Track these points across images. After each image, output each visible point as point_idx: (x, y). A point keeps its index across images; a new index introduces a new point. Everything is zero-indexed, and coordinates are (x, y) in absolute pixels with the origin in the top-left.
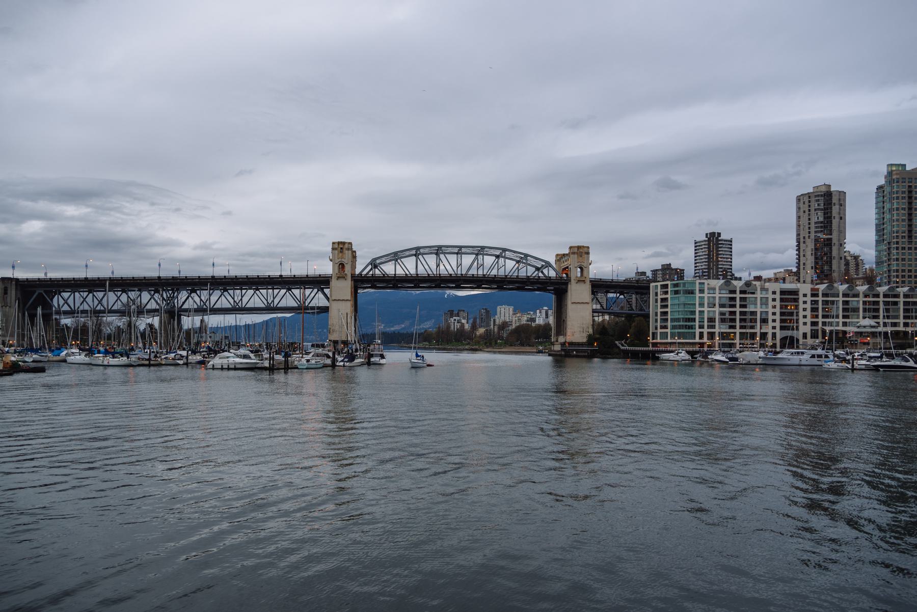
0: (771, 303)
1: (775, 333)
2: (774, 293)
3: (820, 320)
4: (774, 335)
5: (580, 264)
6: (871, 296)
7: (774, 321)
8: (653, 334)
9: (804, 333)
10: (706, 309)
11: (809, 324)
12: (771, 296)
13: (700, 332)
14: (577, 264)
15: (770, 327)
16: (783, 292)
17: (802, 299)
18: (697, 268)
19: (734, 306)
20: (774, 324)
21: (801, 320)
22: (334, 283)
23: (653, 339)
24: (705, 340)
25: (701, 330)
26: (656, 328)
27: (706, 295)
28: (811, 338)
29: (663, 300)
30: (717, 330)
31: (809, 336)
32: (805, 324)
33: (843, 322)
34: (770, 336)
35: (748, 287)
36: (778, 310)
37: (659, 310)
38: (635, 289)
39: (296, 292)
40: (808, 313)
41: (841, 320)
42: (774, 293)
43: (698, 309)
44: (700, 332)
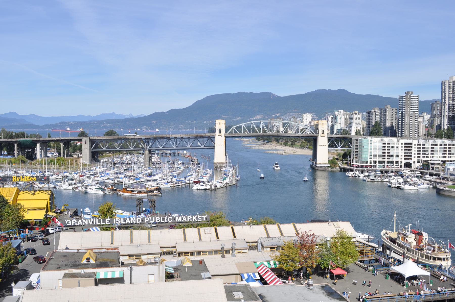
0: (400, 148)
1: (402, 161)
2: (402, 144)
3: (421, 155)
6: (443, 145)
10: (373, 151)
11: (416, 157)
12: (400, 145)
13: (370, 161)
16: (405, 144)
21: (413, 155)
25: (371, 160)
27: (373, 145)
28: (417, 163)
30: (377, 160)
31: (416, 162)
32: (415, 157)
34: (400, 162)
36: (403, 151)
40: (416, 153)
43: (369, 151)
44: (370, 161)
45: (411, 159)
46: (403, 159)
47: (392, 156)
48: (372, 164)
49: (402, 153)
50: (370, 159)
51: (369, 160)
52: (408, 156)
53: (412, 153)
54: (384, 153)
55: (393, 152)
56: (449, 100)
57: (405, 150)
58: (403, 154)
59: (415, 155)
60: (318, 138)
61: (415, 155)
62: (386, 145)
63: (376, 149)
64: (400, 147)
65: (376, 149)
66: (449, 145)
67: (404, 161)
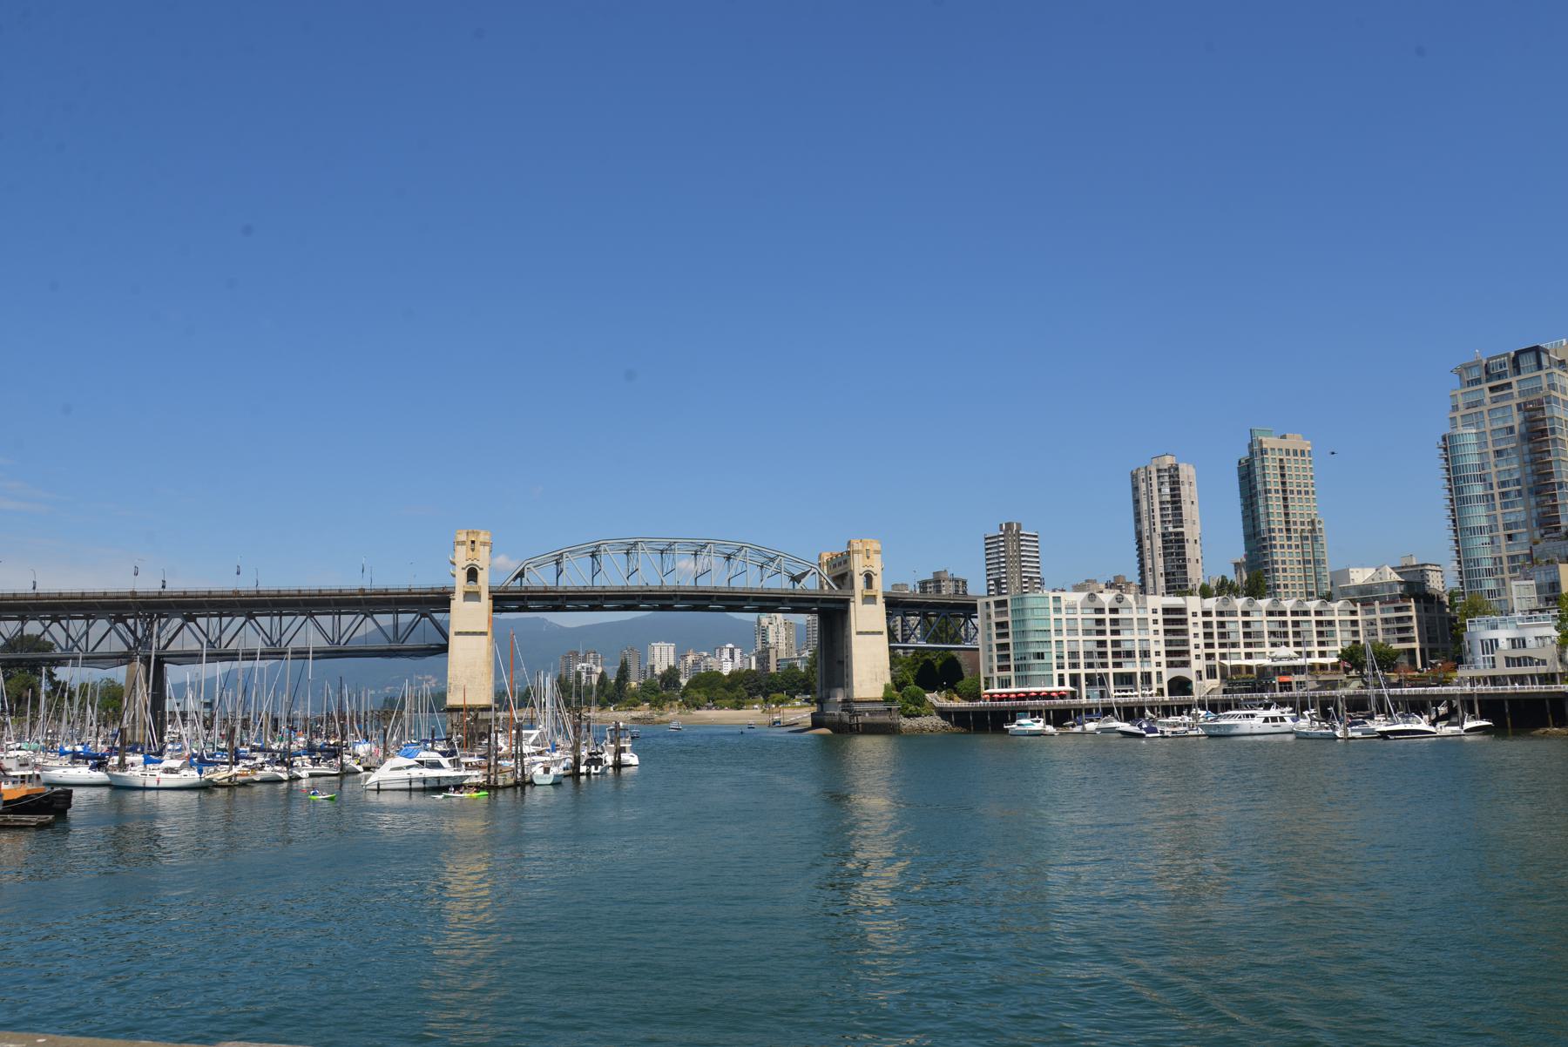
0: (1152, 627)
2: (1155, 611)
4: (1159, 674)
5: (866, 568)
7: (1158, 653)
8: (987, 679)
9: (1197, 672)
10: (1065, 638)
14: (862, 570)
15: (1154, 664)
16: (1166, 611)
17: (1191, 620)
18: (991, 577)
19: (1102, 632)
20: (1158, 659)
22: (457, 603)
23: (987, 688)
24: (1067, 687)
25: (1061, 671)
26: (991, 670)
27: (1063, 616)
29: (1000, 625)
33: (1220, 654)
35: (1120, 602)
36: (1161, 637)
37: (995, 641)
38: (949, 608)
39: (326, 621)
40: (1201, 641)
41: (1243, 650)
42: (1155, 611)
43: (1054, 638)
44: (1059, 675)
45: (1186, 664)
46: (1164, 664)
47: (1130, 654)
48: (1067, 687)
49: (1158, 643)
50: (1058, 668)
51: (1056, 672)
52: (1177, 655)
53: (1188, 645)
54: (1102, 643)
55: (1131, 638)
56: (1163, 522)
57: (1166, 632)
58: (1162, 648)
59: (1198, 652)
60: (852, 605)
61: (1198, 652)
62: (1107, 616)
63: (1075, 631)
64: (1150, 622)
65: (1075, 631)
66: (1294, 613)
67: (1168, 674)
